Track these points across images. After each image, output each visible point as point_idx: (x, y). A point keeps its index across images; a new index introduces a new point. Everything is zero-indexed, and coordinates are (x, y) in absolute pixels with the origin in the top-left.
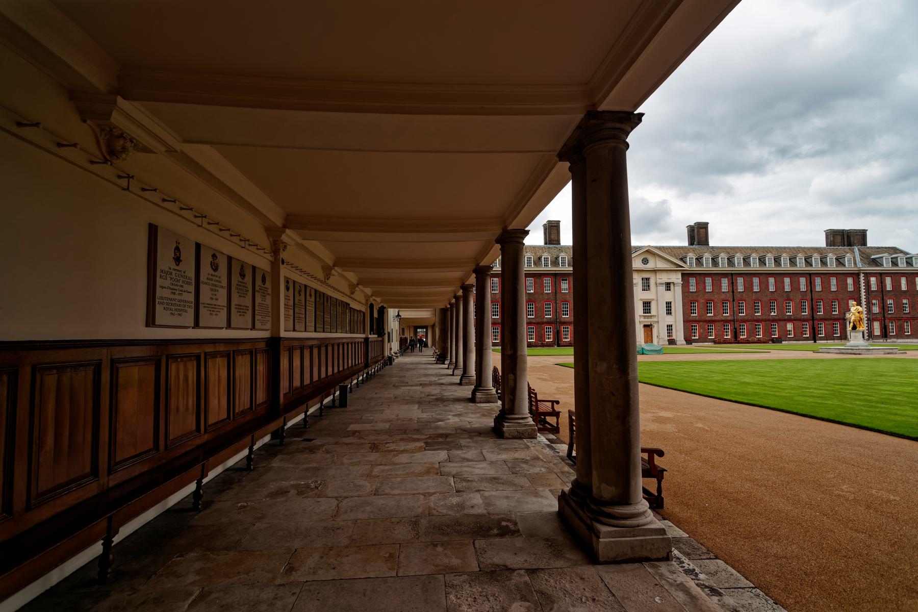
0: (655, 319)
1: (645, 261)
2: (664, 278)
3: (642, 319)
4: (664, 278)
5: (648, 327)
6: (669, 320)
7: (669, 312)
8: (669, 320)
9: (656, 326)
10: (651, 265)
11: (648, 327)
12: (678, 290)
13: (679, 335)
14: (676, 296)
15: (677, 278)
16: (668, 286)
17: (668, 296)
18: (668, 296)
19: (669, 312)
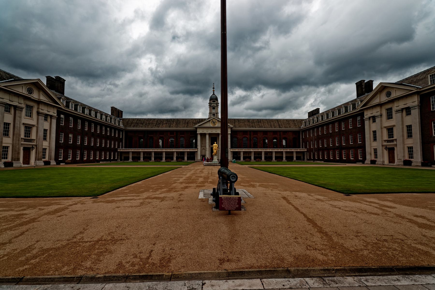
0: (395, 143)
1: (389, 94)
2: (401, 105)
3: (385, 144)
4: (401, 105)
5: (391, 151)
6: (409, 142)
7: (410, 135)
8: (409, 142)
9: (395, 148)
10: (394, 95)
11: (391, 151)
12: (415, 113)
13: (418, 158)
14: (414, 119)
15: (414, 102)
16: (408, 111)
17: (408, 120)
18: (408, 120)
19: (410, 135)
